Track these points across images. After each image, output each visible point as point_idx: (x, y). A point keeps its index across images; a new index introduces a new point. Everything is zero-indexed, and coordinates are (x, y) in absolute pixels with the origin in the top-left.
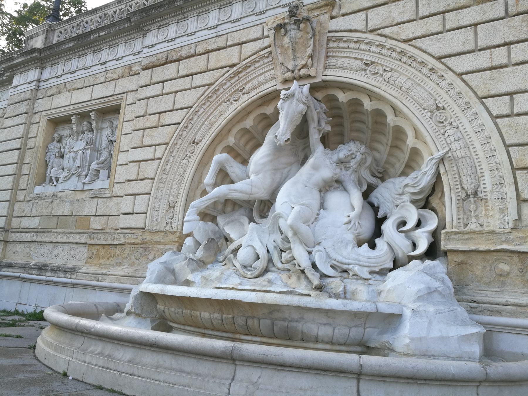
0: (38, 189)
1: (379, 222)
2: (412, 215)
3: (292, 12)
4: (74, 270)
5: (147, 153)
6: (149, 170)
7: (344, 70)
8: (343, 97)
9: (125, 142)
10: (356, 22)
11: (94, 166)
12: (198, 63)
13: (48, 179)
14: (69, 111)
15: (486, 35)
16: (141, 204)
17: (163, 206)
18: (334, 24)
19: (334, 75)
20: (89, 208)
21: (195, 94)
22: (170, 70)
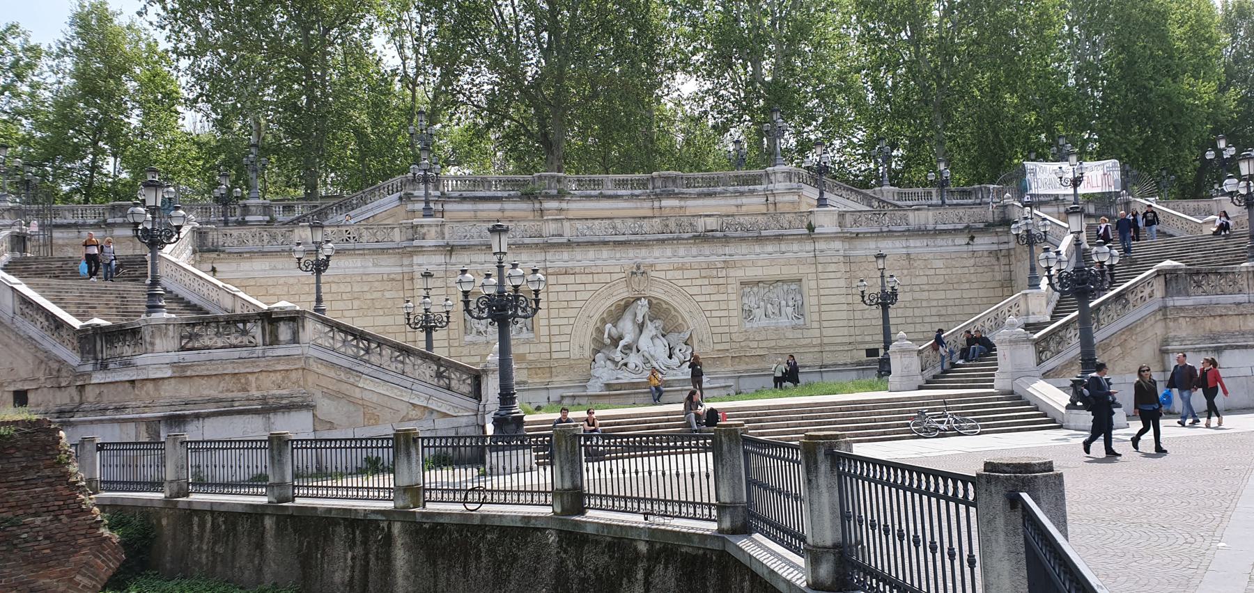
0: (468, 338)
3: (638, 268)
4: (525, 383)
5: (565, 321)
6: (567, 330)
7: (657, 292)
8: (654, 301)
10: (662, 275)
13: (474, 331)
15: (706, 290)
16: (565, 346)
18: (653, 274)
21: (589, 294)
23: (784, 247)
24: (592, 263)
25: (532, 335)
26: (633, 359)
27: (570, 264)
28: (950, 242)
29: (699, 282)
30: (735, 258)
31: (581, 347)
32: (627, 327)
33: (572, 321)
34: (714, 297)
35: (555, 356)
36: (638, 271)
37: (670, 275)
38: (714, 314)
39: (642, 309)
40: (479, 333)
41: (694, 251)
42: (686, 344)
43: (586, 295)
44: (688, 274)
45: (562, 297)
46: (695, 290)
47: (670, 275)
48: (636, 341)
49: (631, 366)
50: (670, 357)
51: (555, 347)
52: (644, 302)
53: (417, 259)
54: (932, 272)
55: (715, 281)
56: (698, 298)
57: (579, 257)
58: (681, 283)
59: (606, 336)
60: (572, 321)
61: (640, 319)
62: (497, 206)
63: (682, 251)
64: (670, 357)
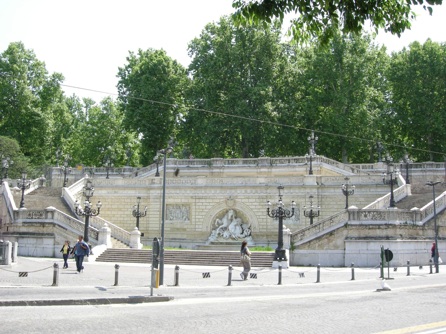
1: (243, 230)
2: (248, 230)
3: (230, 197)
4: (185, 239)
5: (201, 217)
6: (202, 220)
7: (238, 208)
8: (238, 211)
9: (193, 214)
10: (240, 200)
11: (184, 217)
12: (210, 201)
14: (174, 203)
16: (201, 226)
17: (205, 227)
18: (236, 200)
19: (236, 208)
20: (185, 227)
22: (204, 201)
23: (292, 191)
24: (213, 195)
25: (189, 222)
26: (226, 234)
27: (205, 195)
28: (368, 190)
29: (255, 204)
30: (271, 194)
31: (207, 227)
32: (225, 222)
33: (204, 217)
34: (261, 210)
35: (197, 230)
36: (230, 198)
37: (243, 201)
38: (261, 217)
39: (231, 213)
40: (171, 219)
41: (254, 191)
42: (249, 229)
43: (210, 207)
44: (251, 200)
45: (201, 207)
46: (253, 207)
47: (243, 201)
48: (228, 226)
49: (224, 236)
50: (242, 233)
51: (197, 227)
52: (232, 211)
53: (152, 191)
54: (359, 203)
55: (262, 204)
56: (254, 210)
57: (208, 192)
58: (248, 204)
59: (216, 223)
60: (204, 217)
61: (229, 218)
62: (197, 171)
63: (249, 191)
64: (241, 234)
